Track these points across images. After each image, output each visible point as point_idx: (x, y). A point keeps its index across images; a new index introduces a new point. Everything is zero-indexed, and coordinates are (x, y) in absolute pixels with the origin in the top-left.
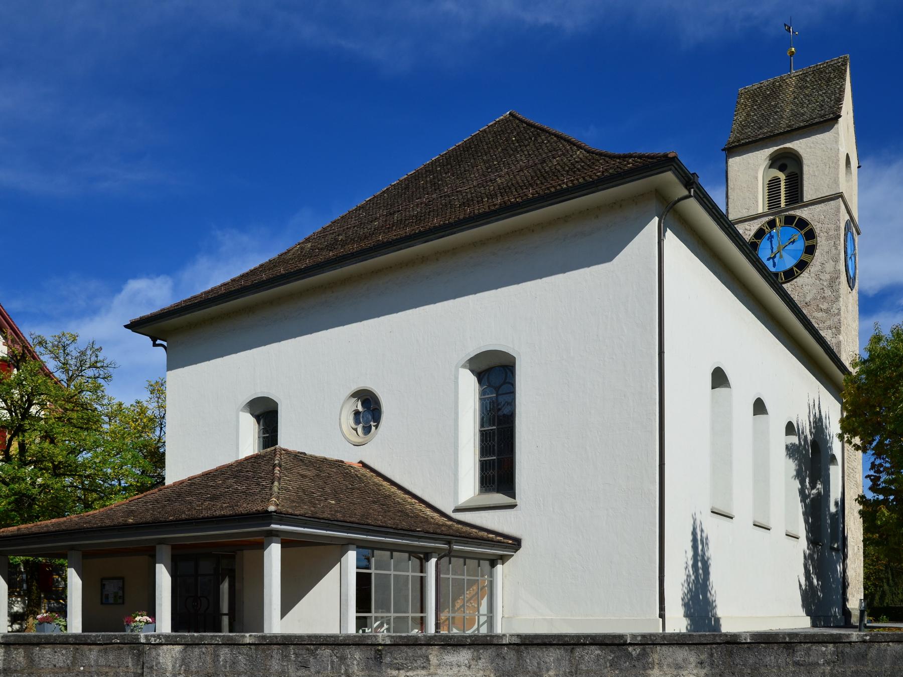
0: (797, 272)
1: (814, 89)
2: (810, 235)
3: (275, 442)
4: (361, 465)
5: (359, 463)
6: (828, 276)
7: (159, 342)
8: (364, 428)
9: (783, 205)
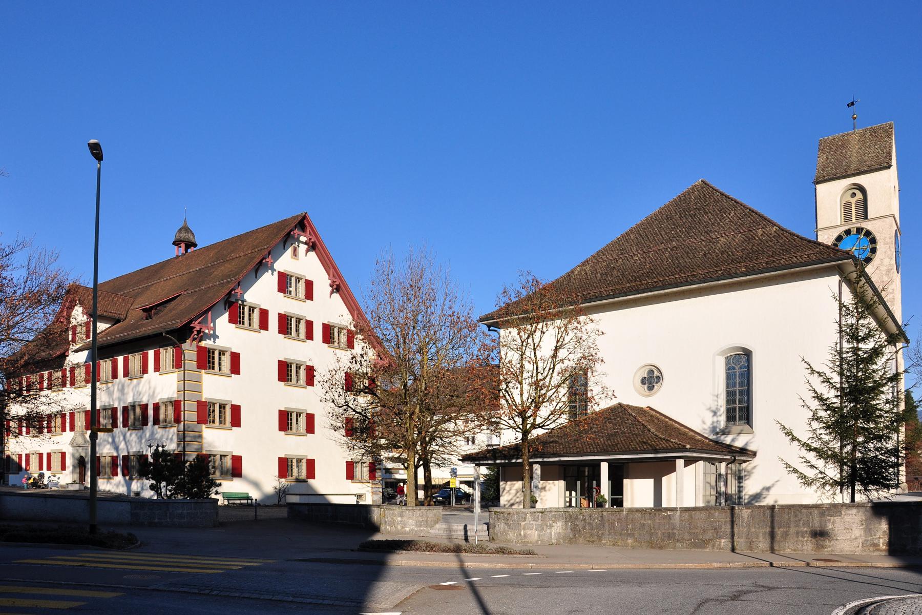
0: (865, 265)
2: (873, 241)
5: (647, 407)
6: (885, 268)
7: (492, 328)
8: (648, 387)
9: (854, 220)
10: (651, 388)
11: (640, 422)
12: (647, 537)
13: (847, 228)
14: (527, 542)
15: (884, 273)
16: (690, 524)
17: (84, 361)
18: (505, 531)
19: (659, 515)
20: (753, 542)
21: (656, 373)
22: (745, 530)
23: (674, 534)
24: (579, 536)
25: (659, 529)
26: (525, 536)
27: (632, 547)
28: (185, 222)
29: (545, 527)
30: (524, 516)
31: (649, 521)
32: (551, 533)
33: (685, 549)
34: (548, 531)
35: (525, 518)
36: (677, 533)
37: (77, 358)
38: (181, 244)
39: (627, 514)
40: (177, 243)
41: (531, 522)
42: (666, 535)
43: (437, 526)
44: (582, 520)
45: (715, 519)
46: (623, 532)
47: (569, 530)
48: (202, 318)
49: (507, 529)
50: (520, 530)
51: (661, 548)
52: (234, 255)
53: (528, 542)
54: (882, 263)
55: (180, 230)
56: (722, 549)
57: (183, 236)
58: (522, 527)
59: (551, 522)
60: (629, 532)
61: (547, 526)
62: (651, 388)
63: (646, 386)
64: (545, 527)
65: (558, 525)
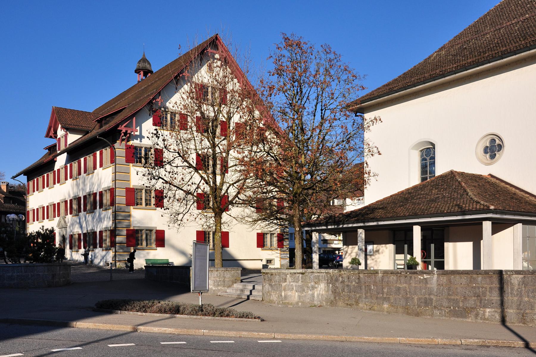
4: (490, 176)
5: (489, 175)
11: (462, 187)
12: (403, 302)
14: (287, 303)
16: (449, 289)
17: (64, 164)
18: (268, 292)
19: (415, 278)
20: (527, 314)
21: (498, 142)
22: (515, 299)
23: (431, 300)
24: (339, 299)
25: (415, 294)
26: (286, 297)
27: (387, 312)
28: (144, 55)
29: (306, 289)
30: (284, 277)
31: (405, 285)
32: (313, 295)
33: (444, 318)
34: (310, 292)
35: (285, 279)
36: (434, 299)
37: (61, 161)
38: (140, 72)
39: (383, 276)
40: (137, 71)
41: (292, 283)
42: (423, 301)
43: (235, 286)
44: (341, 282)
45: (477, 285)
46: (379, 296)
47: (330, 292)
48: (128, 122)
49: (270, 289)
50: (281, 291)
51: (417, 315)
53: (288, 303)
55: (140, 61)
56: (487, 319)
57: (142, 65)
58: (283, 289)
59: (313, 283)
60: (385, 296)
61: (308, 287)
62: (493, 157)
63: (488, 155)
64: (306, 289)
65: (321, 286)
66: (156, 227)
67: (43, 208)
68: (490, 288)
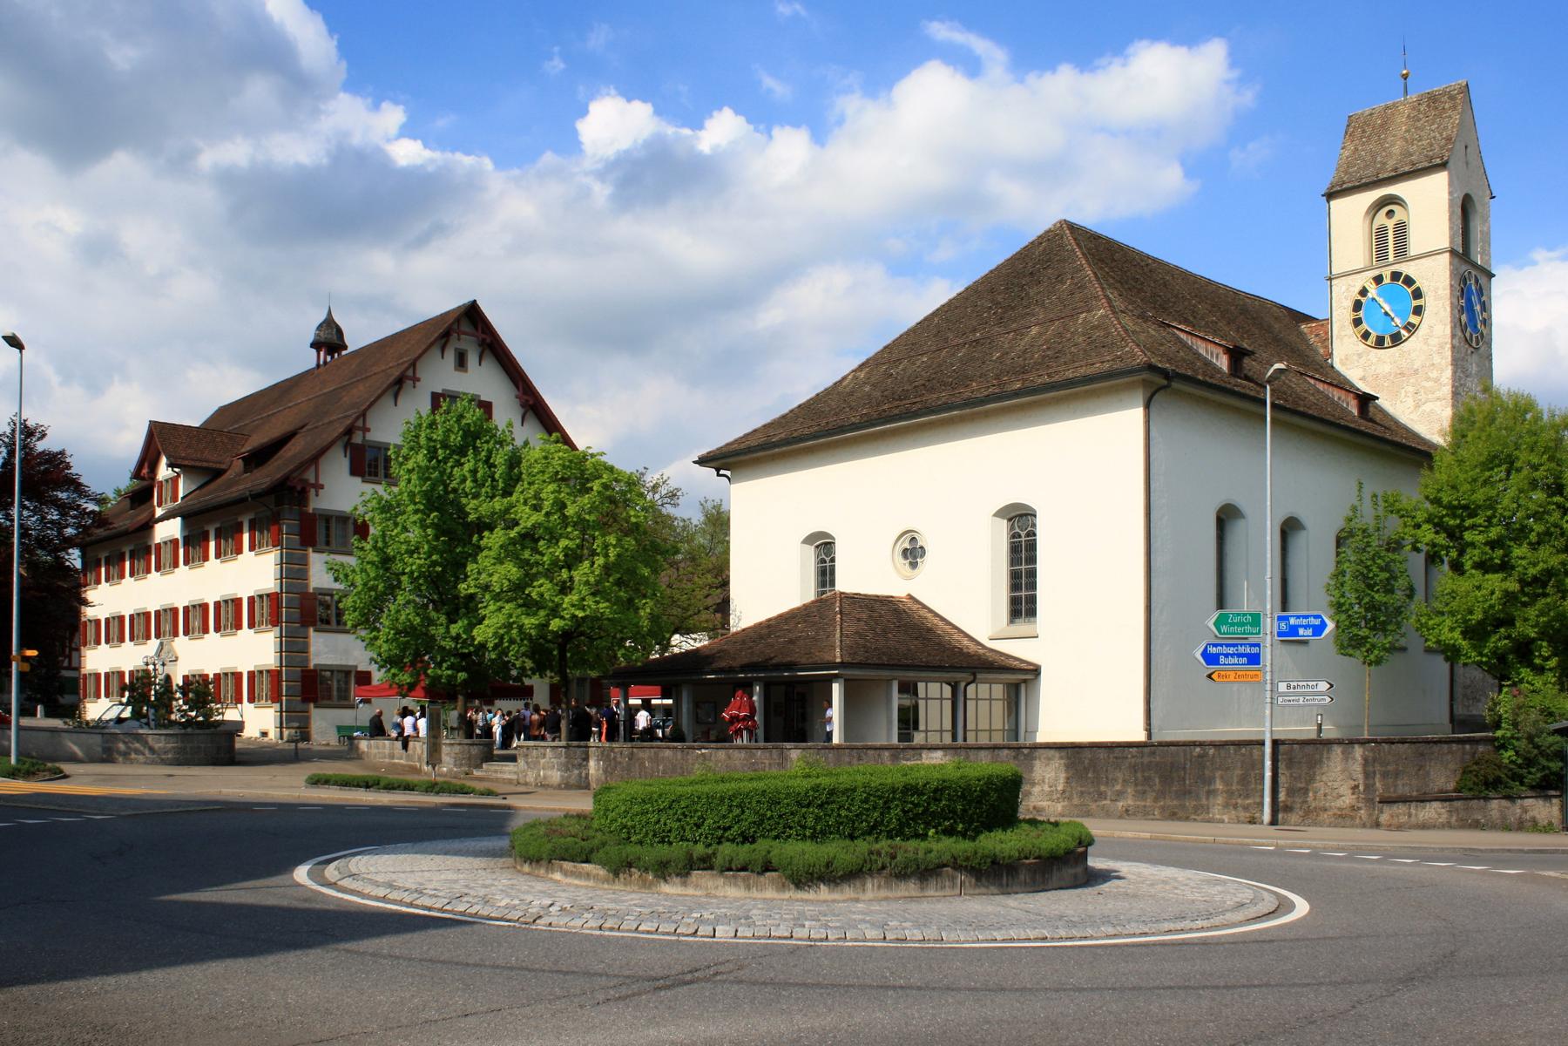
1: (1427, 121)
3: (833, 583)
9: (1391, 258)
10: (914, 565)
13: (1376, 273)
15: (1434, 349)
34: (576, 772)
37: (168, 530)
40: (316, 345)
47: (601, 772)
52: (376, 369)
54: (1432, 332)
55: (321, 325)
62: (914, 565)
66: (356, 667)
67: (121, 618)
68: (770, 764)
